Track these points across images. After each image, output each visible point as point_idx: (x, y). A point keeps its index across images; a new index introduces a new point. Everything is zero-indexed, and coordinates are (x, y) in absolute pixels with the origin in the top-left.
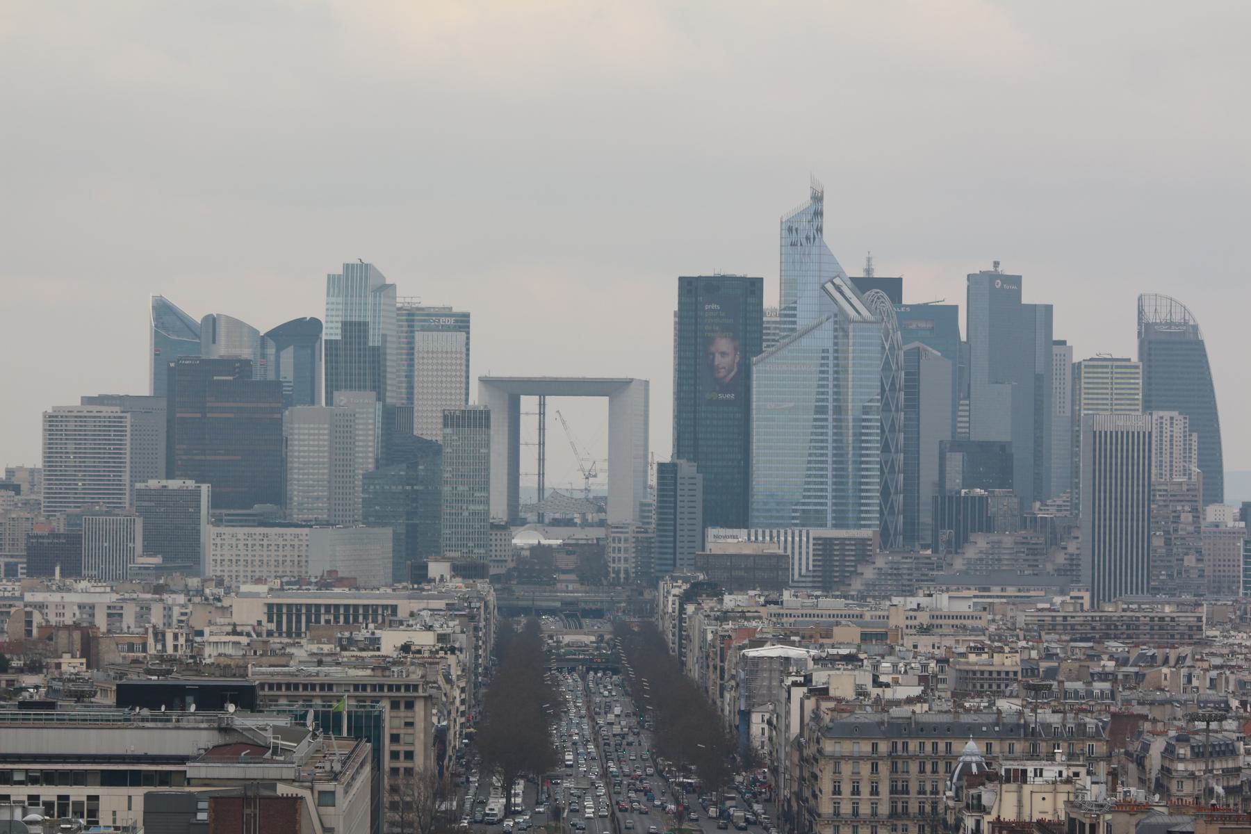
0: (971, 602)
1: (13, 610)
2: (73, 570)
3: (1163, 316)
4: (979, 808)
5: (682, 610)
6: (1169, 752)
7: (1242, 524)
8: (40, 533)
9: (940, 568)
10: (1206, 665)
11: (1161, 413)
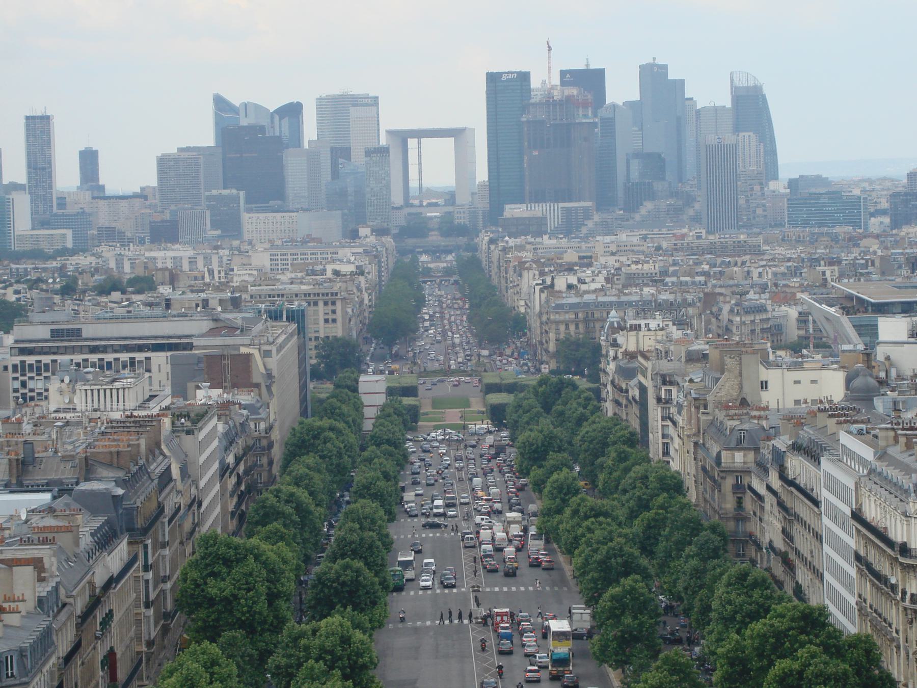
2: (173, 238)
3: (743, 83)
4: (615, 344)
5: (489, 249)
6: (732, 311)
7: (788, 190)
9: (628, 220)
10: (757, 265)
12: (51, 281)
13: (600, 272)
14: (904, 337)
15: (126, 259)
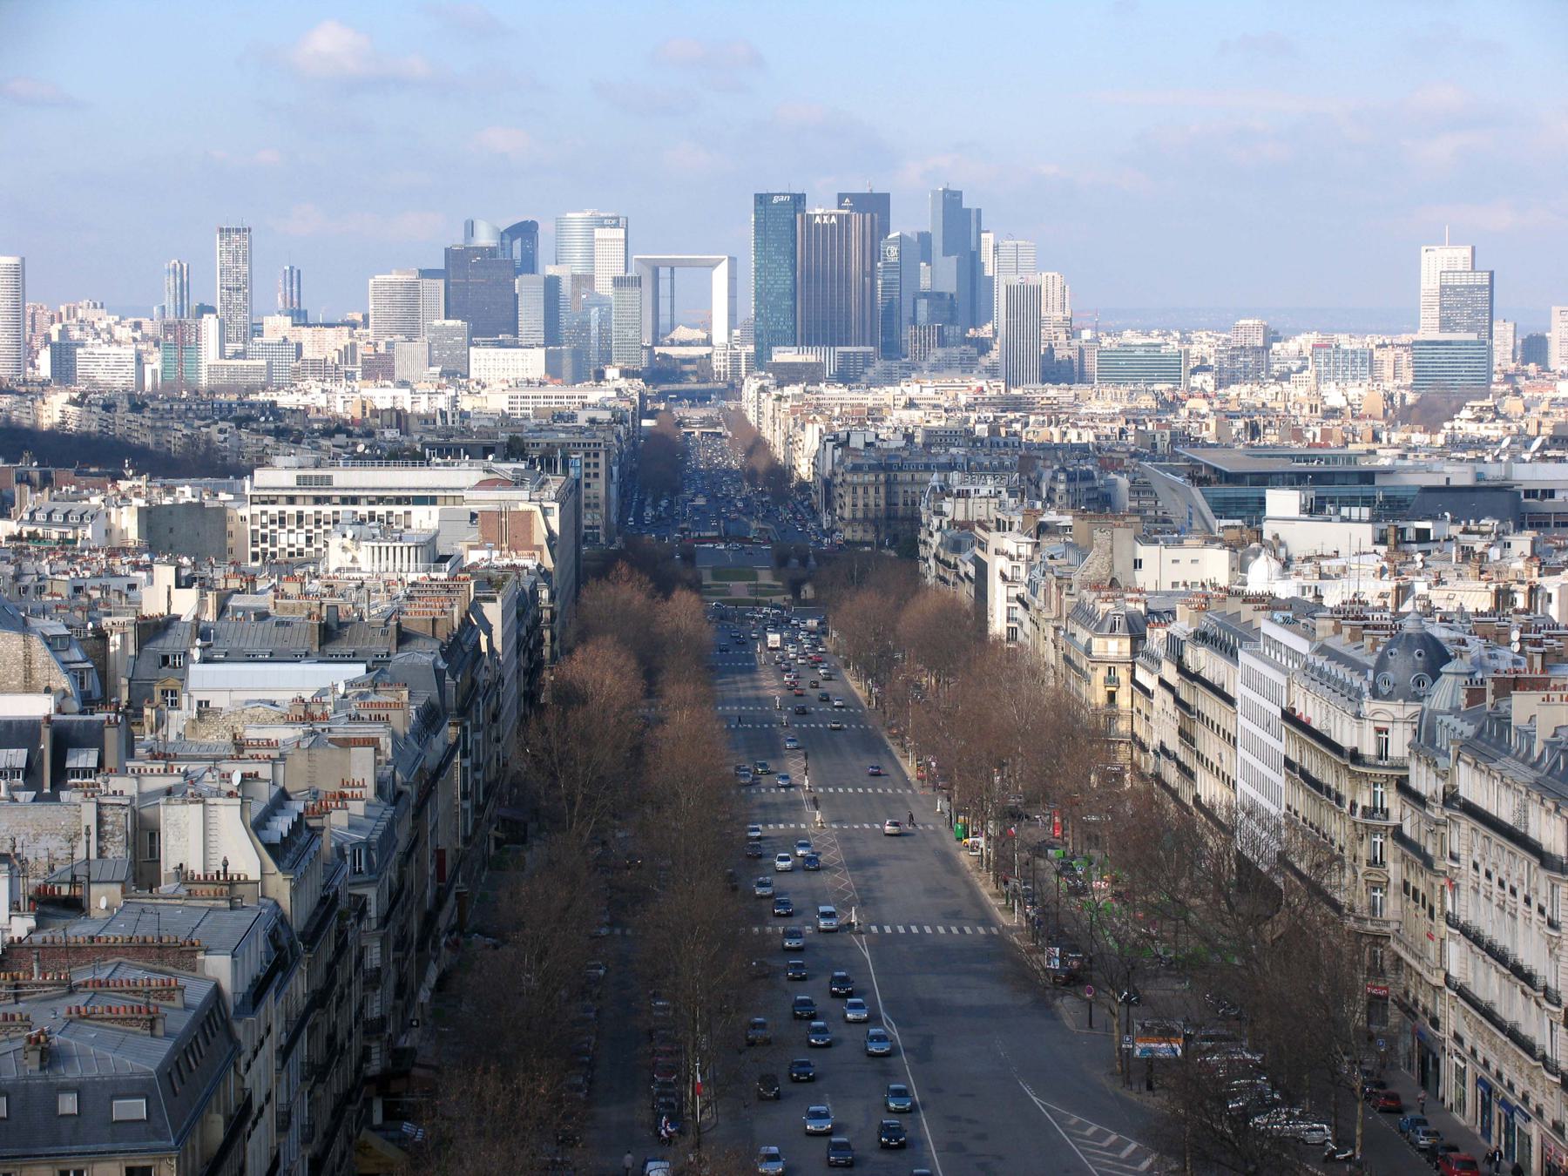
4: (940, 513)
5: (759, 397)
6: (1054, 478)
12: (263, 419)
14: (1295, 513)
15: (338, 396)
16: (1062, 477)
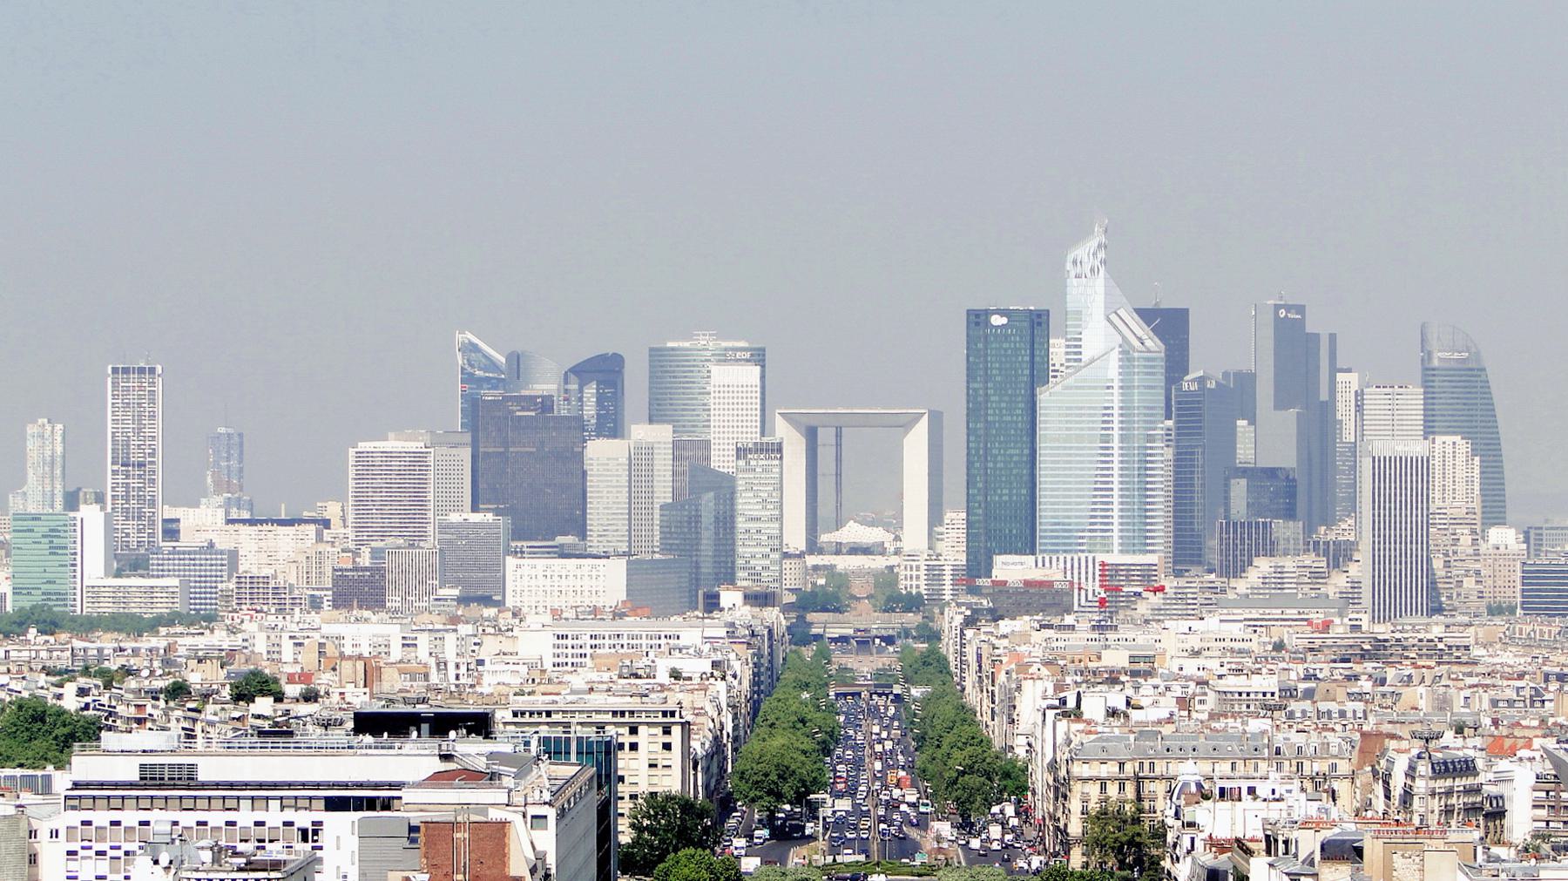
0: (1241, 625)
1: (306, 642)
8: (345, 567)
11: (1444, 438)
13: (1168, 689)
15: (285, 636)
16: (1423, 768)
